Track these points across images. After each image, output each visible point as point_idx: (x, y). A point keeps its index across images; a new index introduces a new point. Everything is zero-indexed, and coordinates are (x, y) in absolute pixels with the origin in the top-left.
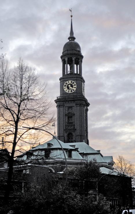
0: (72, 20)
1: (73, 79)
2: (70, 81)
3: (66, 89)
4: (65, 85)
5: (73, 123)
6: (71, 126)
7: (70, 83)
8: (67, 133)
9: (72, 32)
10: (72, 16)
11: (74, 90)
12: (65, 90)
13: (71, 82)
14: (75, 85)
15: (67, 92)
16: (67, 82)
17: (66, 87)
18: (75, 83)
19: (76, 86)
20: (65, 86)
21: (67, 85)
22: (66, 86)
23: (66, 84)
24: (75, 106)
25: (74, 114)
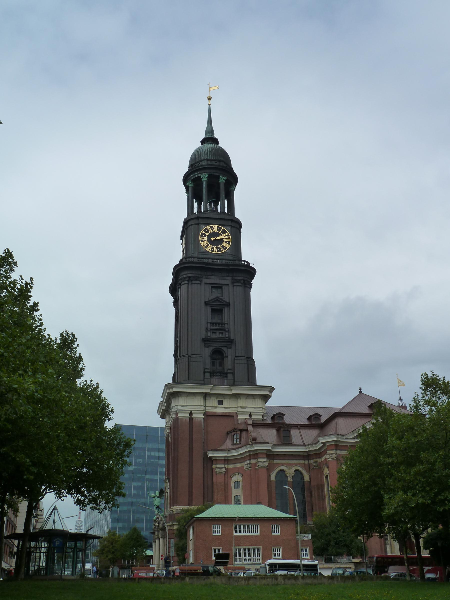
0: (210, 105)
2: (216, 226)
3: (204, 243)
6: (220, 333)
7: (216, 230)
8: (212, 348)
9: (210, 130)
10: (209, 99)
12: (202, 244)
13: (219, 229)
15: (207, 249)
16: (208, 227)
17: (206, 238)
18: (228, 233)
19: (230, 240)
20: (202, 236)
21: (207, 234)
22: (205, 236)
23: (205, 231)
24: (231, 286)
25: (229, 303)
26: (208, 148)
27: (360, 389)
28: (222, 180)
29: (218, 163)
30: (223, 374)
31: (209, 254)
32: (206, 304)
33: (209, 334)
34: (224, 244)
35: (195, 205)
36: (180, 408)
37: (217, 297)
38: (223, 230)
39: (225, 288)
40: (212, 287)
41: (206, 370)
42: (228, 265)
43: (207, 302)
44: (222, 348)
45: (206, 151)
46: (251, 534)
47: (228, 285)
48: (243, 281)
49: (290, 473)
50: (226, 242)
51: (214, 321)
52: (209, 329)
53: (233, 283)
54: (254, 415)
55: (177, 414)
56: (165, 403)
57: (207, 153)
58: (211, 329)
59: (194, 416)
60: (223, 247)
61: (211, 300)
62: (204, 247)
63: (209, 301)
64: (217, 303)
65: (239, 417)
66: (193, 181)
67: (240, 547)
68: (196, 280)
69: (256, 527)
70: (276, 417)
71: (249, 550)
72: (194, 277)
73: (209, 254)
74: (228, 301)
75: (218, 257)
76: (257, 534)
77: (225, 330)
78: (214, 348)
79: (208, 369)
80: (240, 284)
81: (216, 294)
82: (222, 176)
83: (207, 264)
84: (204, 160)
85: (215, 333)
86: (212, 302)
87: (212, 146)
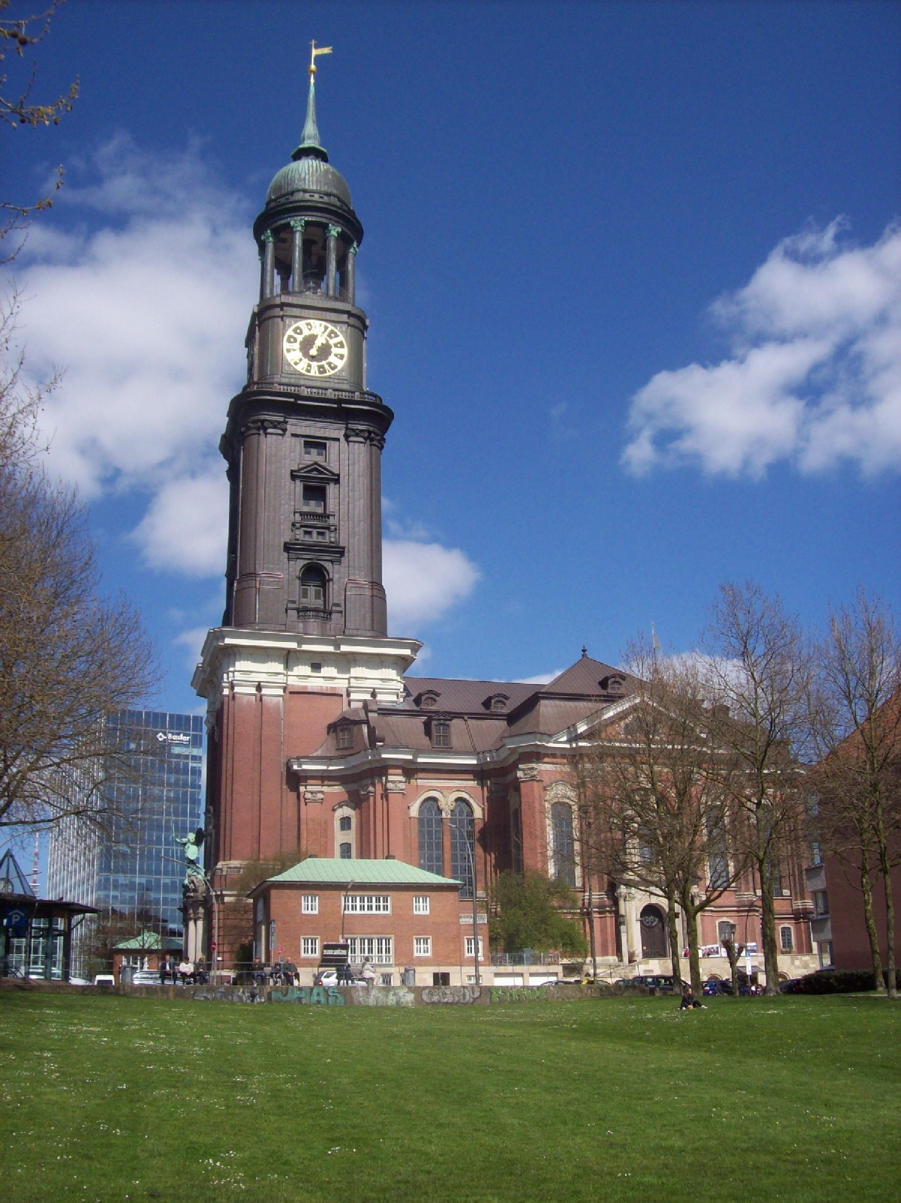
1: (333, 316)
4: (290, 337)
5: (332, 521)
6: (319, 533)
8: (301, 563)
11: (335, 367)
14: (342, 346)
16: (302, 324)
17: (297, 346)
18: (341, 338)
19: (345, 351)
20: (289, 341)
21: (300, 338)
23: (295, 331)
24: (342, 439)
25: (338, 475)
26: (307, 168)
27: (584, 651)
28: (334, 231)
29: (326, 199)
30: (325, 613)
31: (303, 377)
32: (294, 476)
33: (300, 534)
34: (332, 359)
35: (277, 280)
36: (238, 676)
37: (316, 463)
38: (332, 332)
39: (332, 446)
40: (307, 444)
41: (290, 605)
42: (339, 401)
43: (295, 471)
44: (322, 563)
45: (303, 175)
46: (374, 912)
47: (338, 440)
48: (366, 435)
49: (447, 802)
50: (336, 355)
51: (306, 509)
52: (298, 525)
53: (347, 437)
54: (381, 693)
55: (232, 687)
56: (208, 665)
57: (305, 177)
58: (302, 526)
59: (264, 691)
60: (329, 364)
61: (303, 469)
62: (292, 363)
63: (299, 470)
64: (314, 474)
65: (353, 696)
66: (276, 232)
67: (354, 936)
68: (275, 427)
69: (385, 900)
70: (423, 698)
71: (370, 941)
72: (271, 422)
73: (303, 377)
74: (337, 472)
75: (318, 384)
76: (385, 912)
77: (328, 528)
78: (306, 562)
79: (294, 602)
80: (361, 439)
81: (314, 456)
82: (333, 225)
83: (298, 397)
84: (298, 191)
85: (310, 533)
86: (305, 472)
87: (315, 165)
